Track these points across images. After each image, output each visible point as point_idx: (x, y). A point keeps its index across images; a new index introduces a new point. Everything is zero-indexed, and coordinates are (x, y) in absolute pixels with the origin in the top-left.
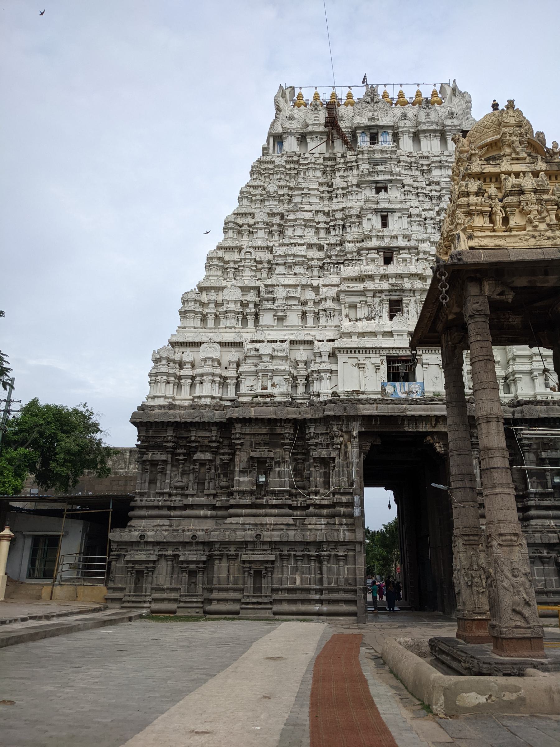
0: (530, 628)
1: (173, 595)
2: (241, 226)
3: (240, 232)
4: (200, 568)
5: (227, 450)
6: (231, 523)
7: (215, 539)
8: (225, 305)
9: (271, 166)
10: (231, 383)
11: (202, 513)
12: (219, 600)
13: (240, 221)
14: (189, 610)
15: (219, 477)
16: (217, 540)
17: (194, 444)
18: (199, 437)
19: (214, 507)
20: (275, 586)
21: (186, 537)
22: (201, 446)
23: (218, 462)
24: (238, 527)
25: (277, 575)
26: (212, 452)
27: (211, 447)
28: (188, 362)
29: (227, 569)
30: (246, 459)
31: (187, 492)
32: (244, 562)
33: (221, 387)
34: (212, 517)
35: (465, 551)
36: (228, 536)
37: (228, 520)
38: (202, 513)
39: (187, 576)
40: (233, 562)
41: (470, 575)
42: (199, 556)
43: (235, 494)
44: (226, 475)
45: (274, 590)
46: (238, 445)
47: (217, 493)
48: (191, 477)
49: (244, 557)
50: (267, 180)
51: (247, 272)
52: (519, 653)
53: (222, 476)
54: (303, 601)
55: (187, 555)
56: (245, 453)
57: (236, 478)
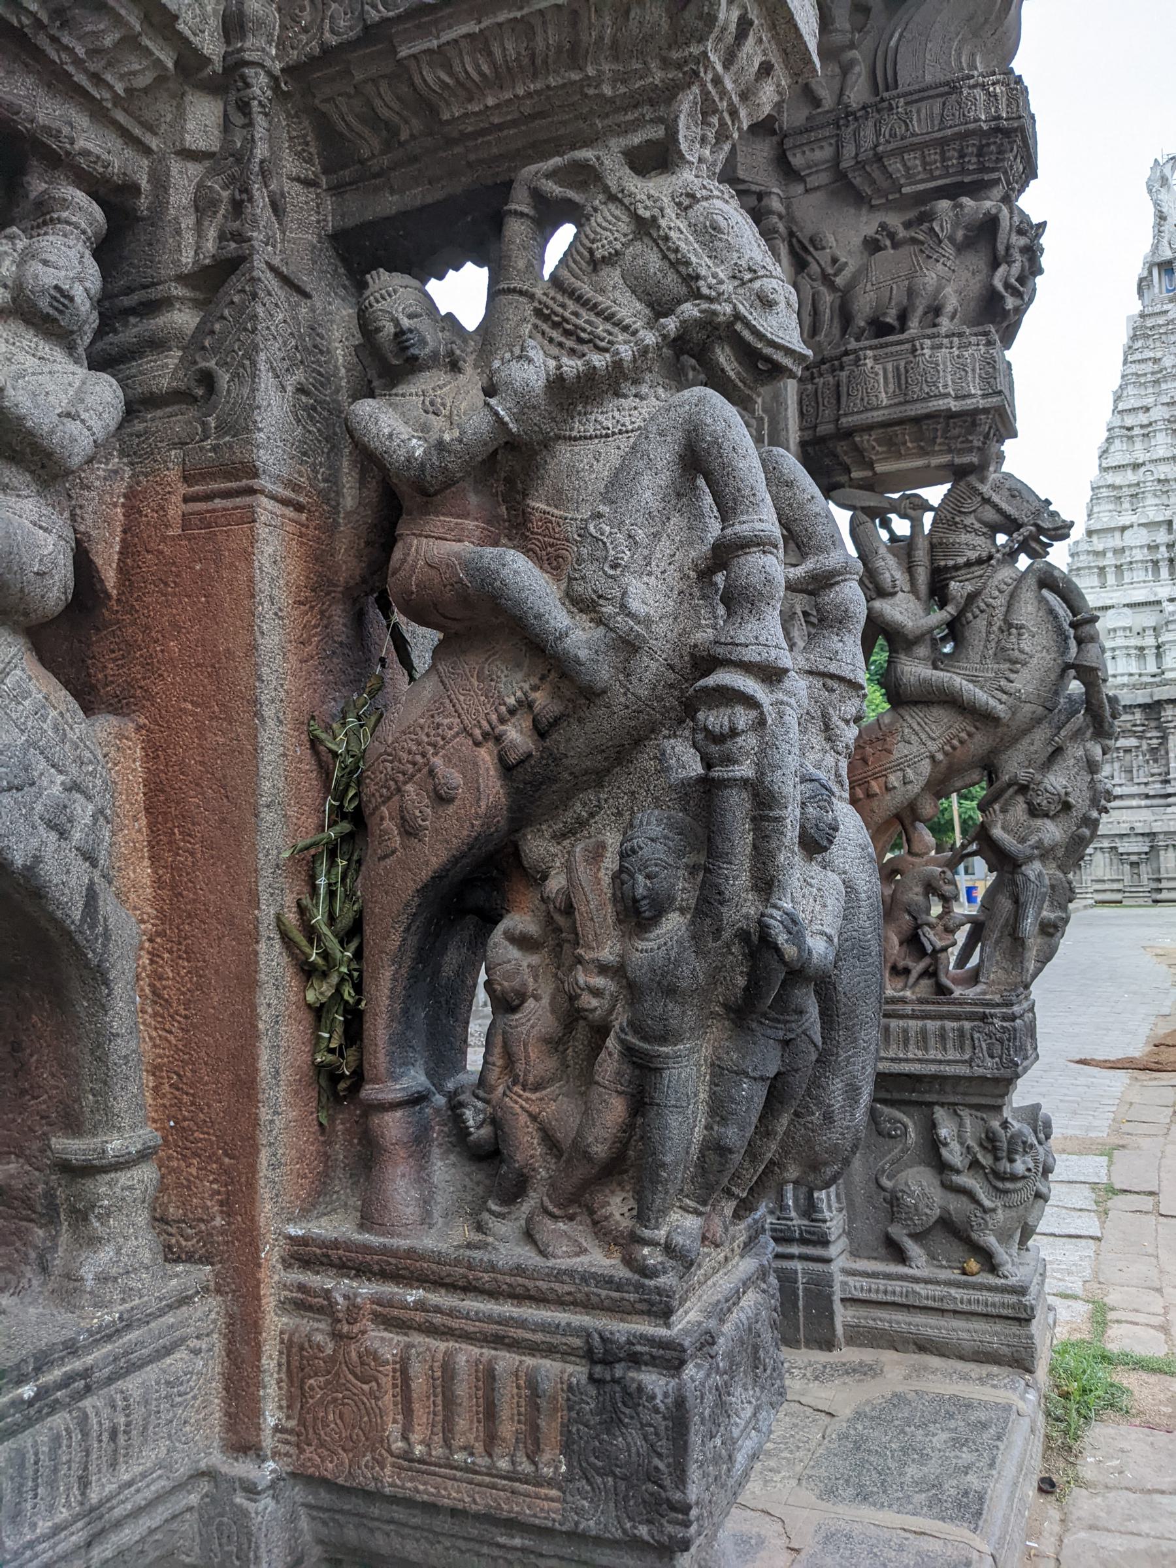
1: (1115, 886)
2: (1129, 429)
3: (1130, 438)
5: (1155, 734)
8: (1127, 553)
9: (1161, 320)
10: (1150, 654)
13: (1129, 421)
19: (1147, 796)
21: (1124, 829)
34: (1147, 807)
37: (1169, 810)
38: (1134, 803)
44: (1156, 761)
48: (1116, 765)
50: (1158, 344)
51: (1151, 500)
55: (1124, 847)
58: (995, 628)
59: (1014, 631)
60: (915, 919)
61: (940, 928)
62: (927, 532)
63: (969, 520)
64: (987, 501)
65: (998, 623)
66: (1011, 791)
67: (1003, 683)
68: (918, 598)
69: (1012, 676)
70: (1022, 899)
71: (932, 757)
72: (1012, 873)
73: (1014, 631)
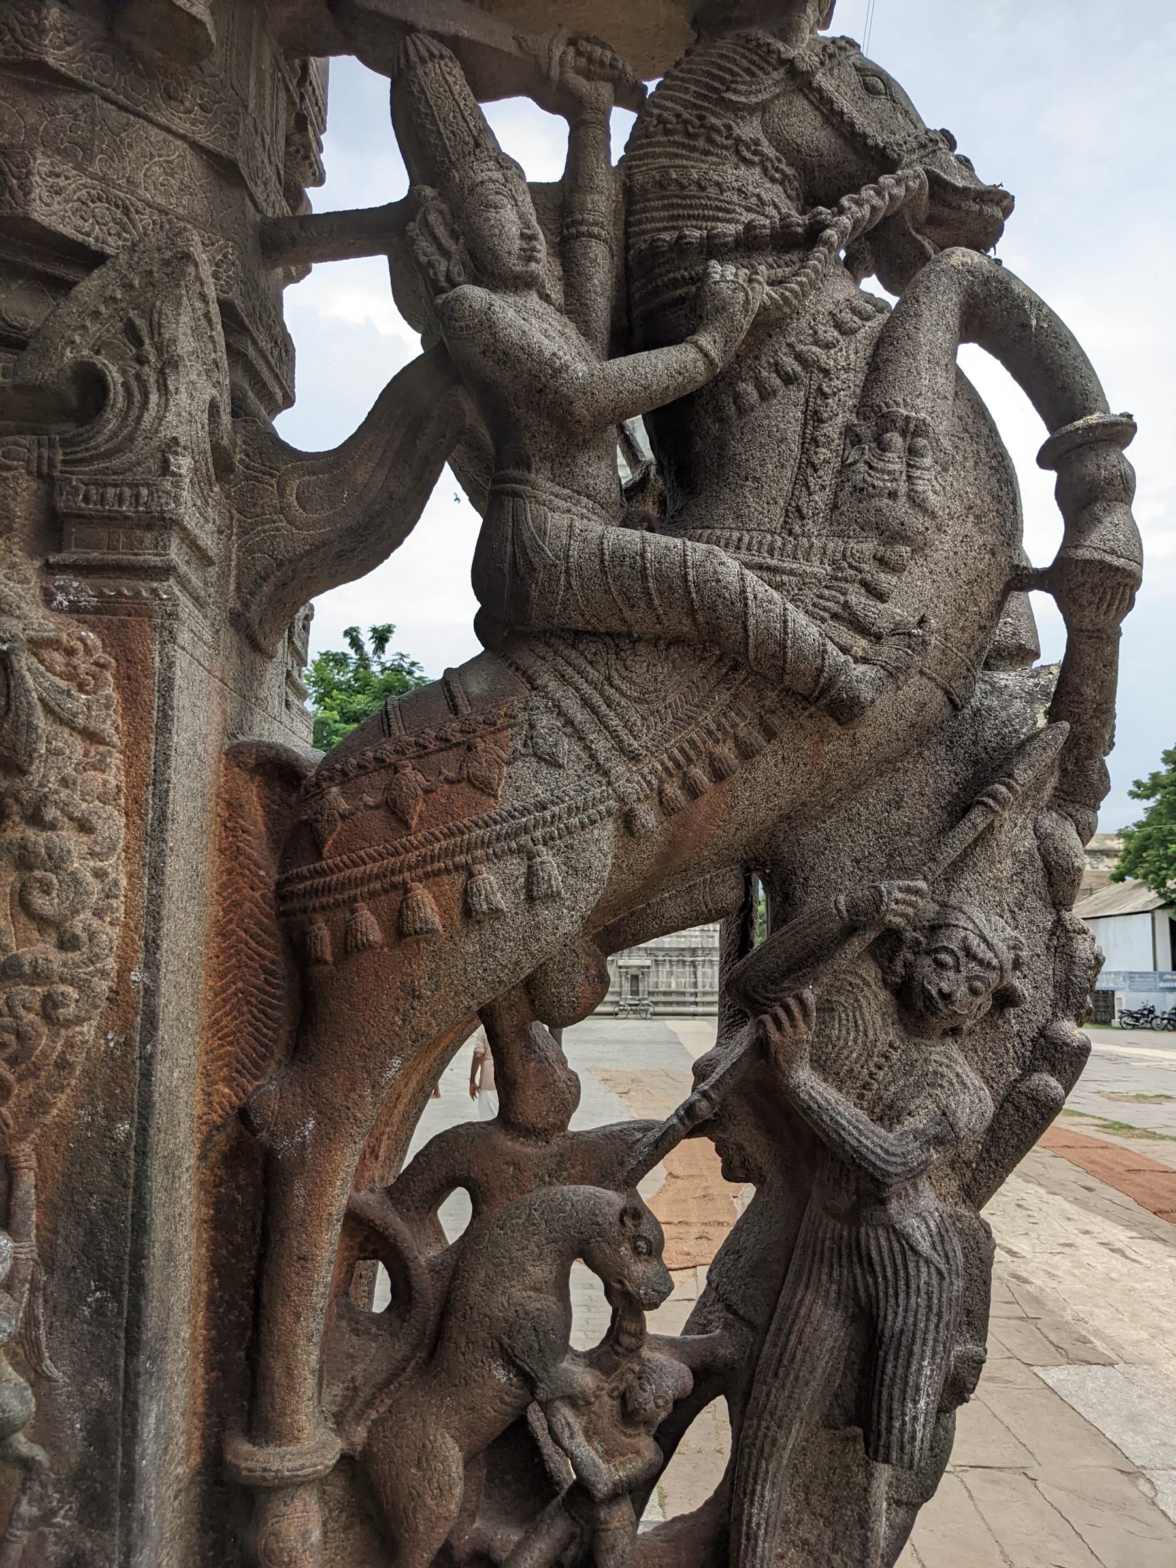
20: (651, 989)
25: (652, 979)
32: (620, 967)
45: (650, 993)
49: (621, 963)
54: (678, 1003)
58: (832, 430)
59: (896, 439)
60: (529, 1381)
61: (607, 1406)
62: (614, 162)
63: (750, 130)
64: (799, 80)
65: (840, 414)
66: (857, 945)
67: (857, 598)
68: (586, 331)
69: (886, 580)
70: (893, 1322)
71: (627, 822)
72: (854, 1217)
73: (896, 439)
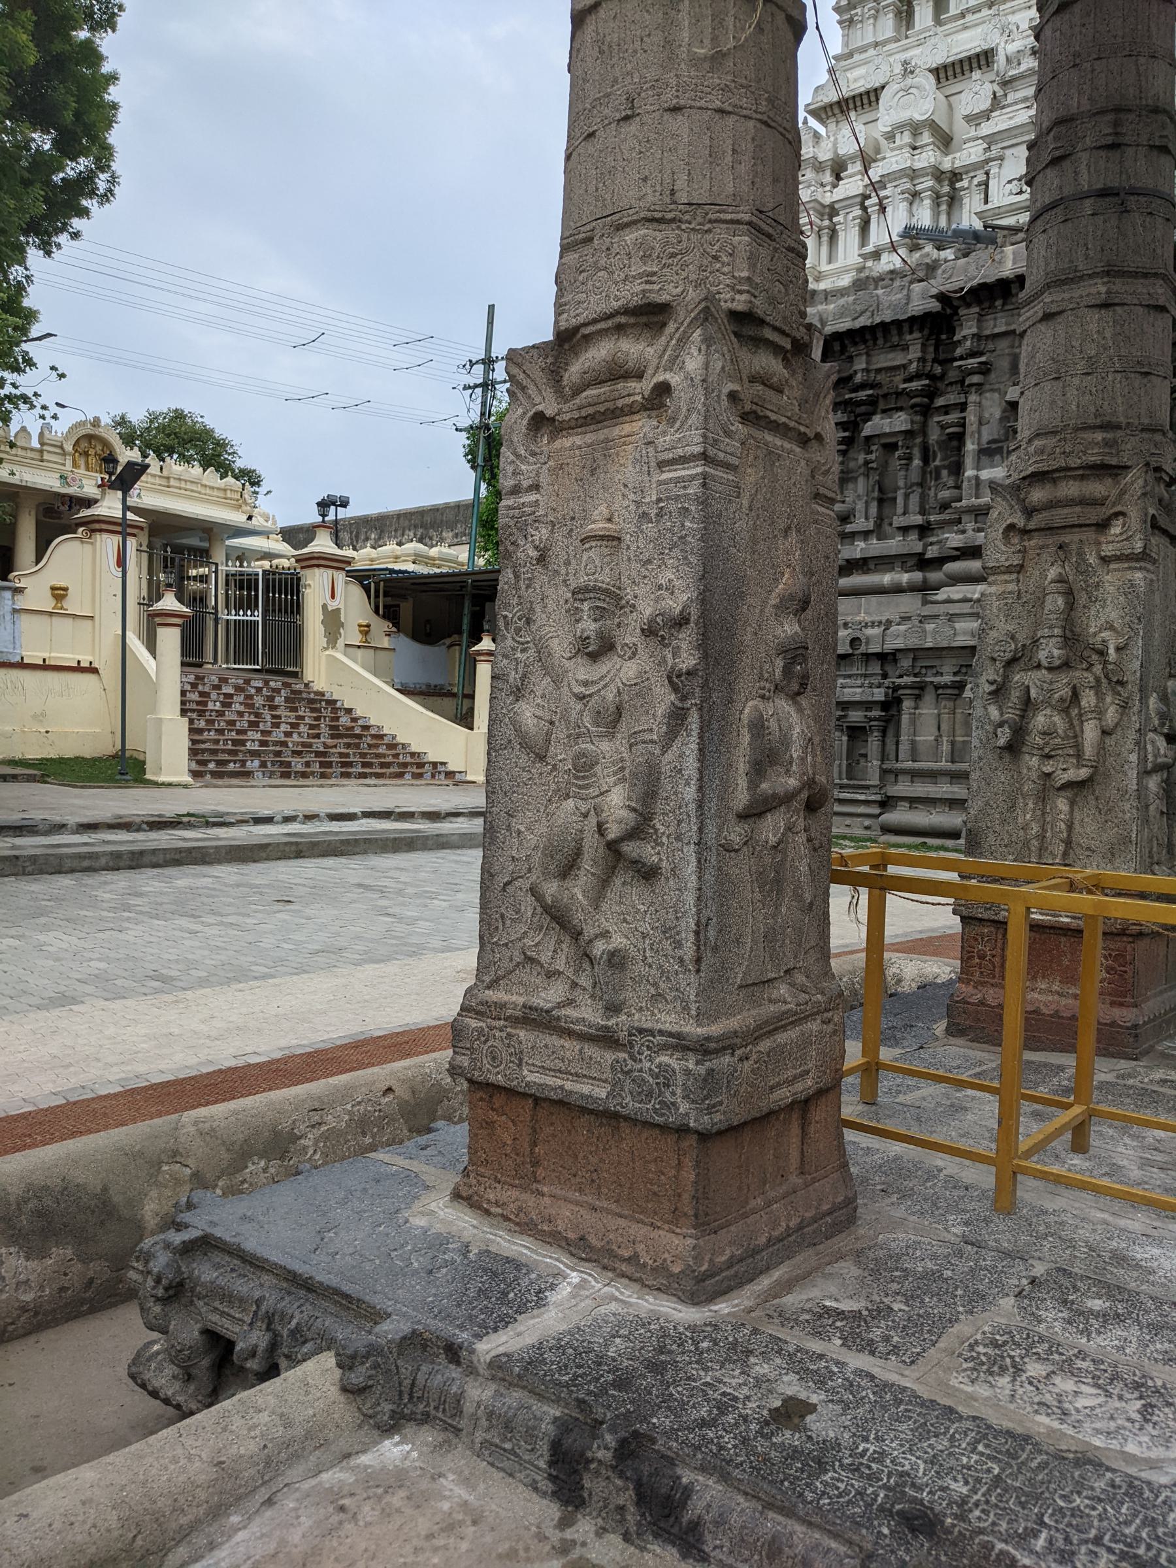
0: (606, 1039)
4: (871, 720)
6: (949, 601)
7: (899, 644)
11: (887, 579)
12: (914, 802)
14: (848, 821)
15: (938, 477)
16: (902, 646)
17: (862, 395)
18: (879, 371)
22: (885, 396)
23: (934, 436)
24: (966, 608)
26: (913, 407)
27: (910, 395)
28: (852, 158)
29: (934, 722)
30: (998, 414)
31: (849, 528)
33: (944, 207)
34: (912, 588)
35: (1021, 568)
36: (933, 635)
38: (887, 579)
39: (845, 738)
40: (950, 704)
41: (1015, 695)
42: (868, 690)
43: (965, 518)
46: (972, 373)
47: (929, 522)
52: (529, 1200)
53: (945, 473)
56: (996, 395)
57: (970, 473)
